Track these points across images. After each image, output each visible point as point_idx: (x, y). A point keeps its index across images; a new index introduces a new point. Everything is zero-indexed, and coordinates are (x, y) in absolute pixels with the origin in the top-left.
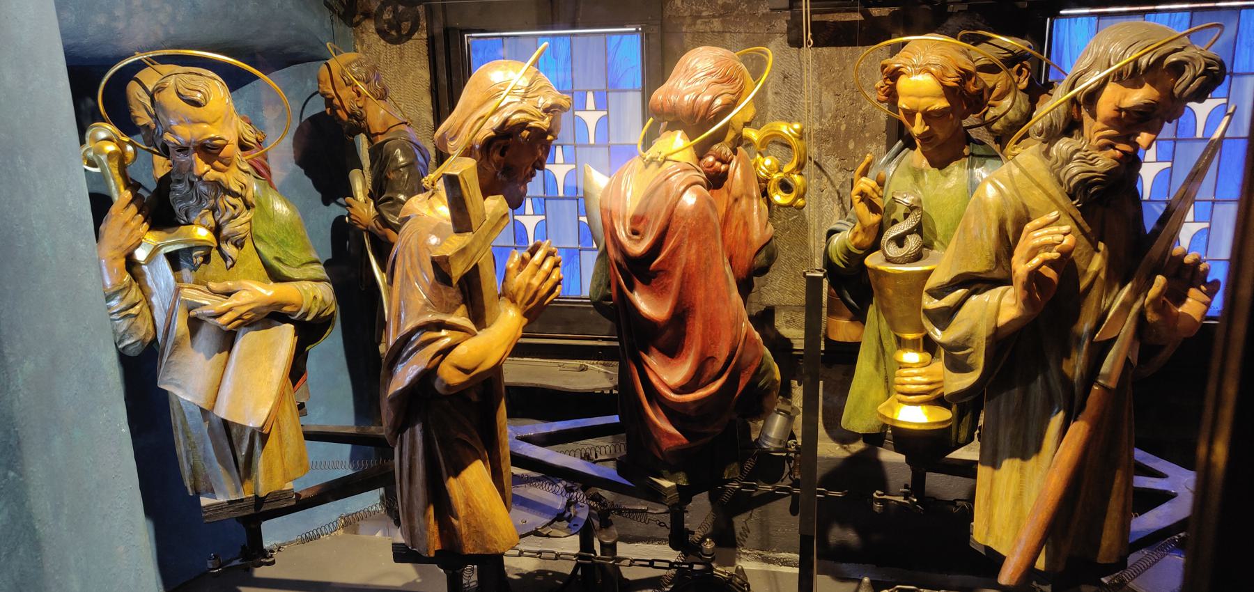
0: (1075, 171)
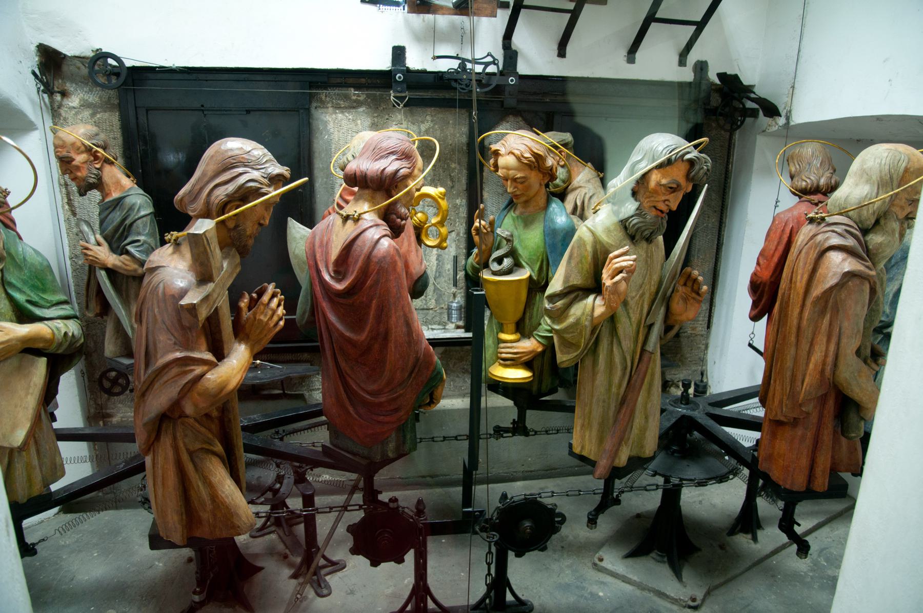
0: (635, 221)
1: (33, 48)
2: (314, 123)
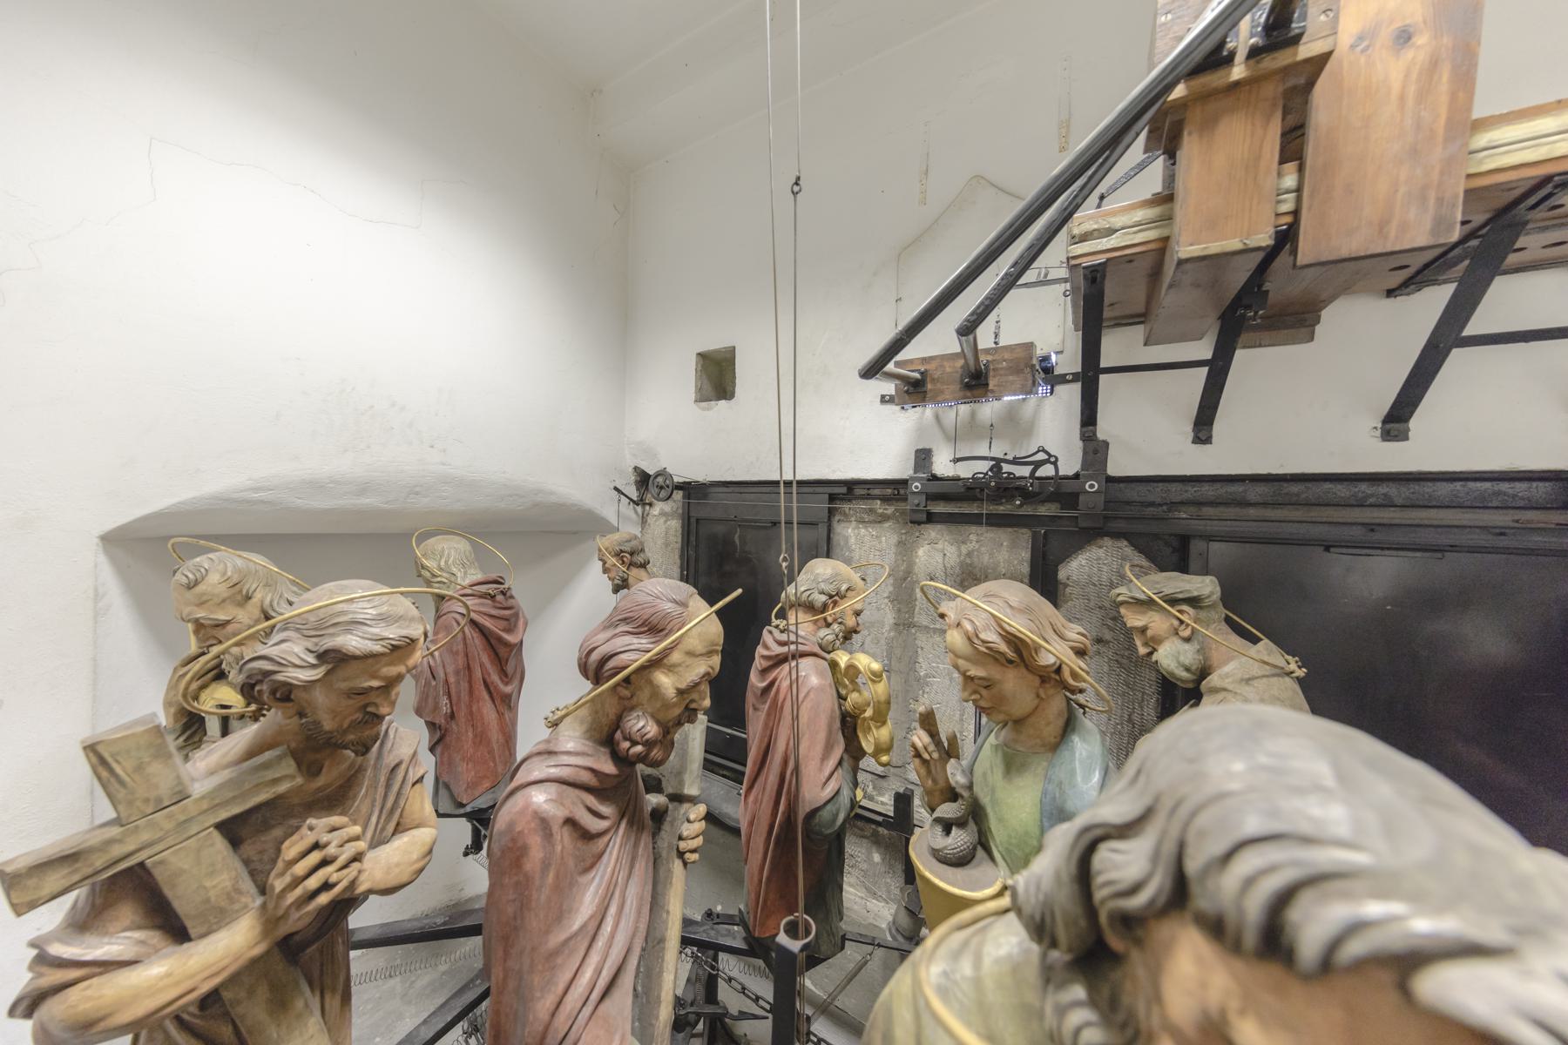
1: (631, 469)
2: (835, 538)
